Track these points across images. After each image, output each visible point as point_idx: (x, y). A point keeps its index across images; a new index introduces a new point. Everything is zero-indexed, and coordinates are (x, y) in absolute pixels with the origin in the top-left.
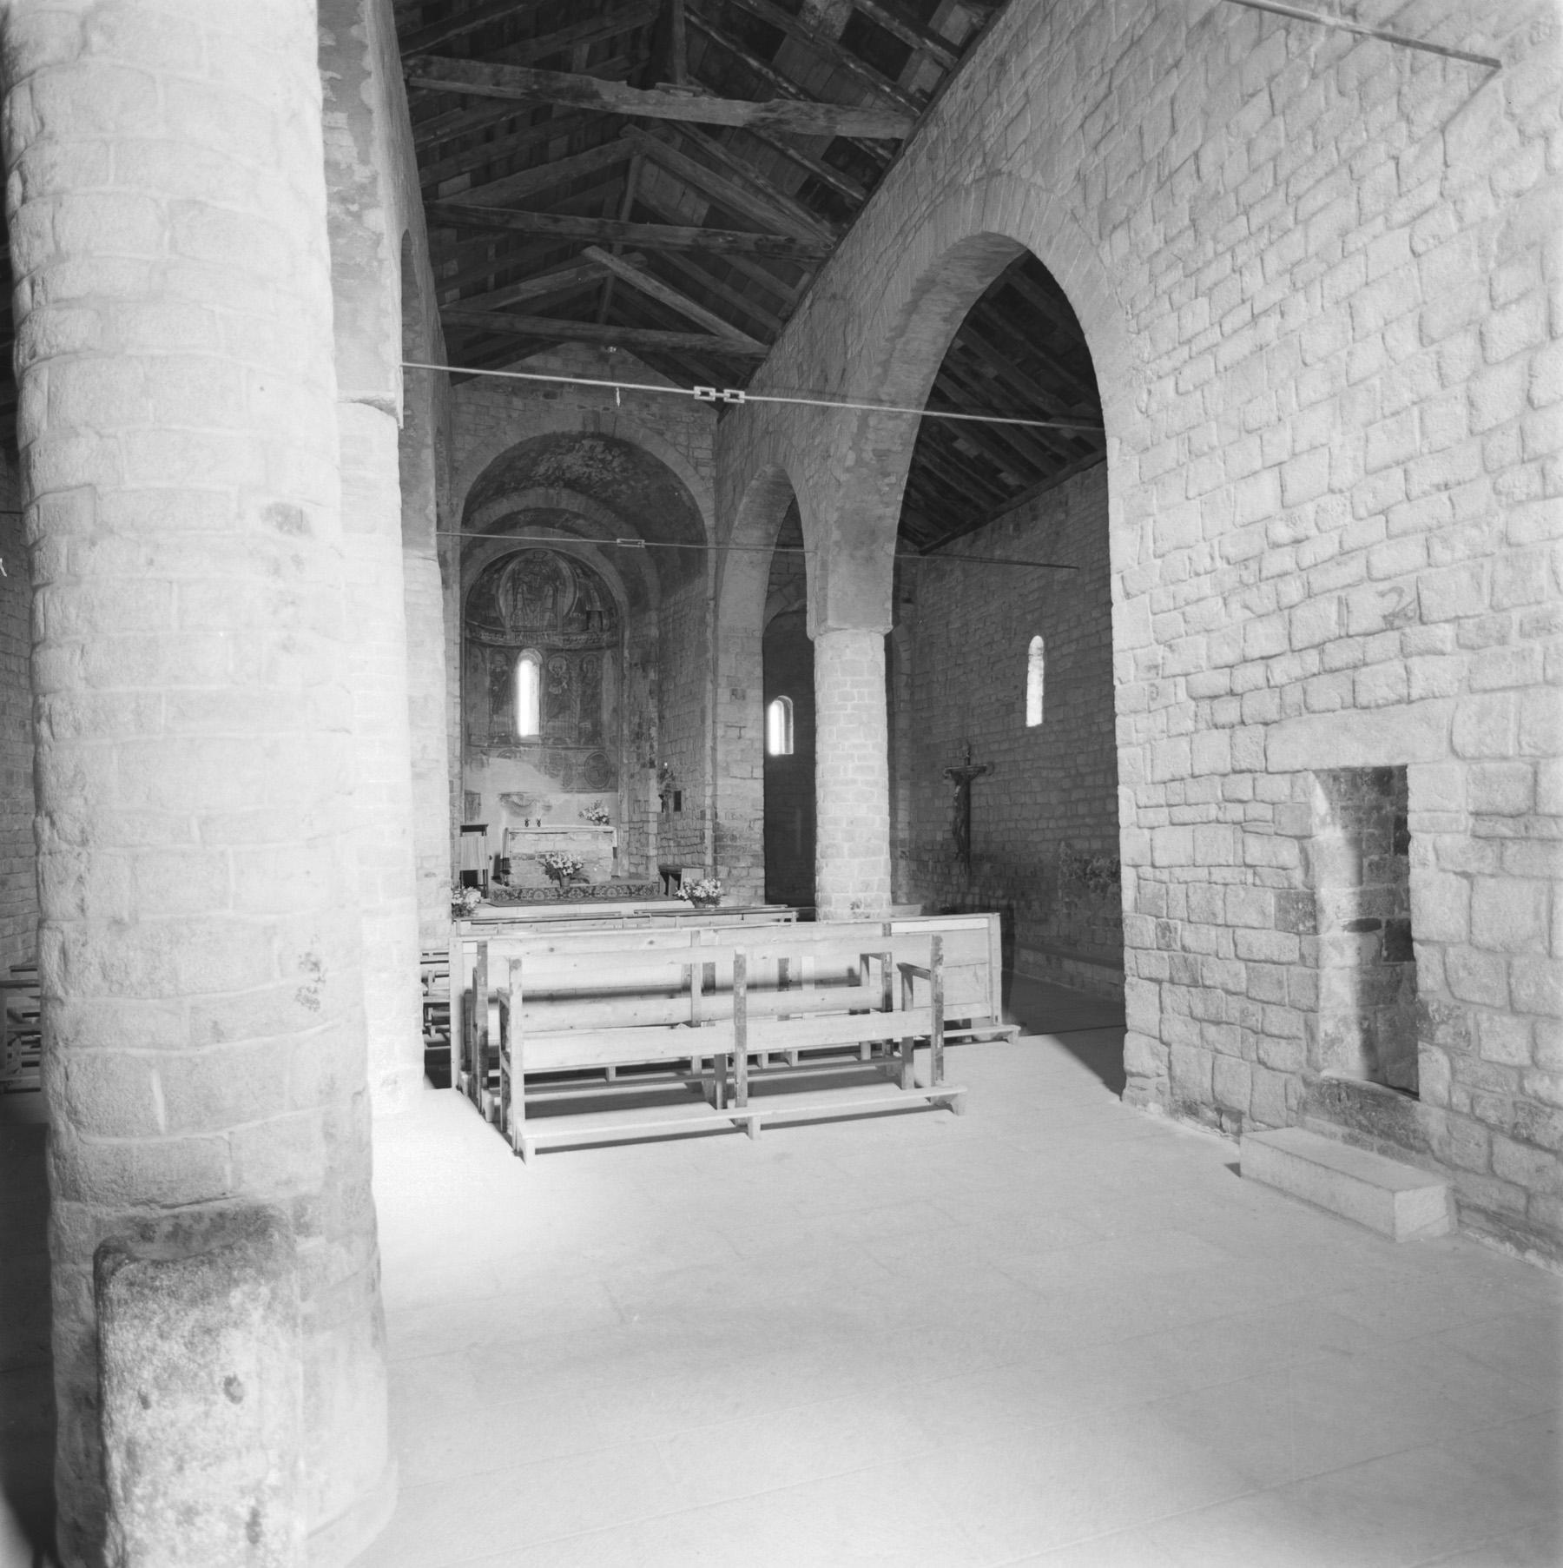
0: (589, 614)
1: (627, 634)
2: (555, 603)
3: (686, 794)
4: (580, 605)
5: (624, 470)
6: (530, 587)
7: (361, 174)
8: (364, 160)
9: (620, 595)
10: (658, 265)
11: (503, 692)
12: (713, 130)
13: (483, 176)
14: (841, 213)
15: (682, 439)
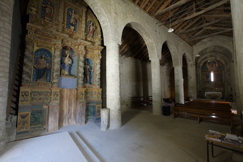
0: (220, 66)
1: (225, 68)
2: (215, 65)
3: (232, 88)
4: (219, 65)
5: (219, 49)
6: (211, 64)
7: (152, 42)
8: (152, 41)
9: (224, 63)
10: (213, 25)
11: (209, 76)
12: (218, 7)
13: (183, 28)
14: (229, 11)
15: (227, 43)
